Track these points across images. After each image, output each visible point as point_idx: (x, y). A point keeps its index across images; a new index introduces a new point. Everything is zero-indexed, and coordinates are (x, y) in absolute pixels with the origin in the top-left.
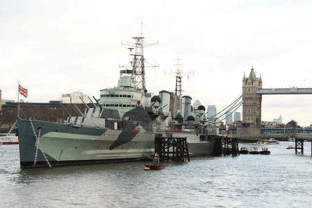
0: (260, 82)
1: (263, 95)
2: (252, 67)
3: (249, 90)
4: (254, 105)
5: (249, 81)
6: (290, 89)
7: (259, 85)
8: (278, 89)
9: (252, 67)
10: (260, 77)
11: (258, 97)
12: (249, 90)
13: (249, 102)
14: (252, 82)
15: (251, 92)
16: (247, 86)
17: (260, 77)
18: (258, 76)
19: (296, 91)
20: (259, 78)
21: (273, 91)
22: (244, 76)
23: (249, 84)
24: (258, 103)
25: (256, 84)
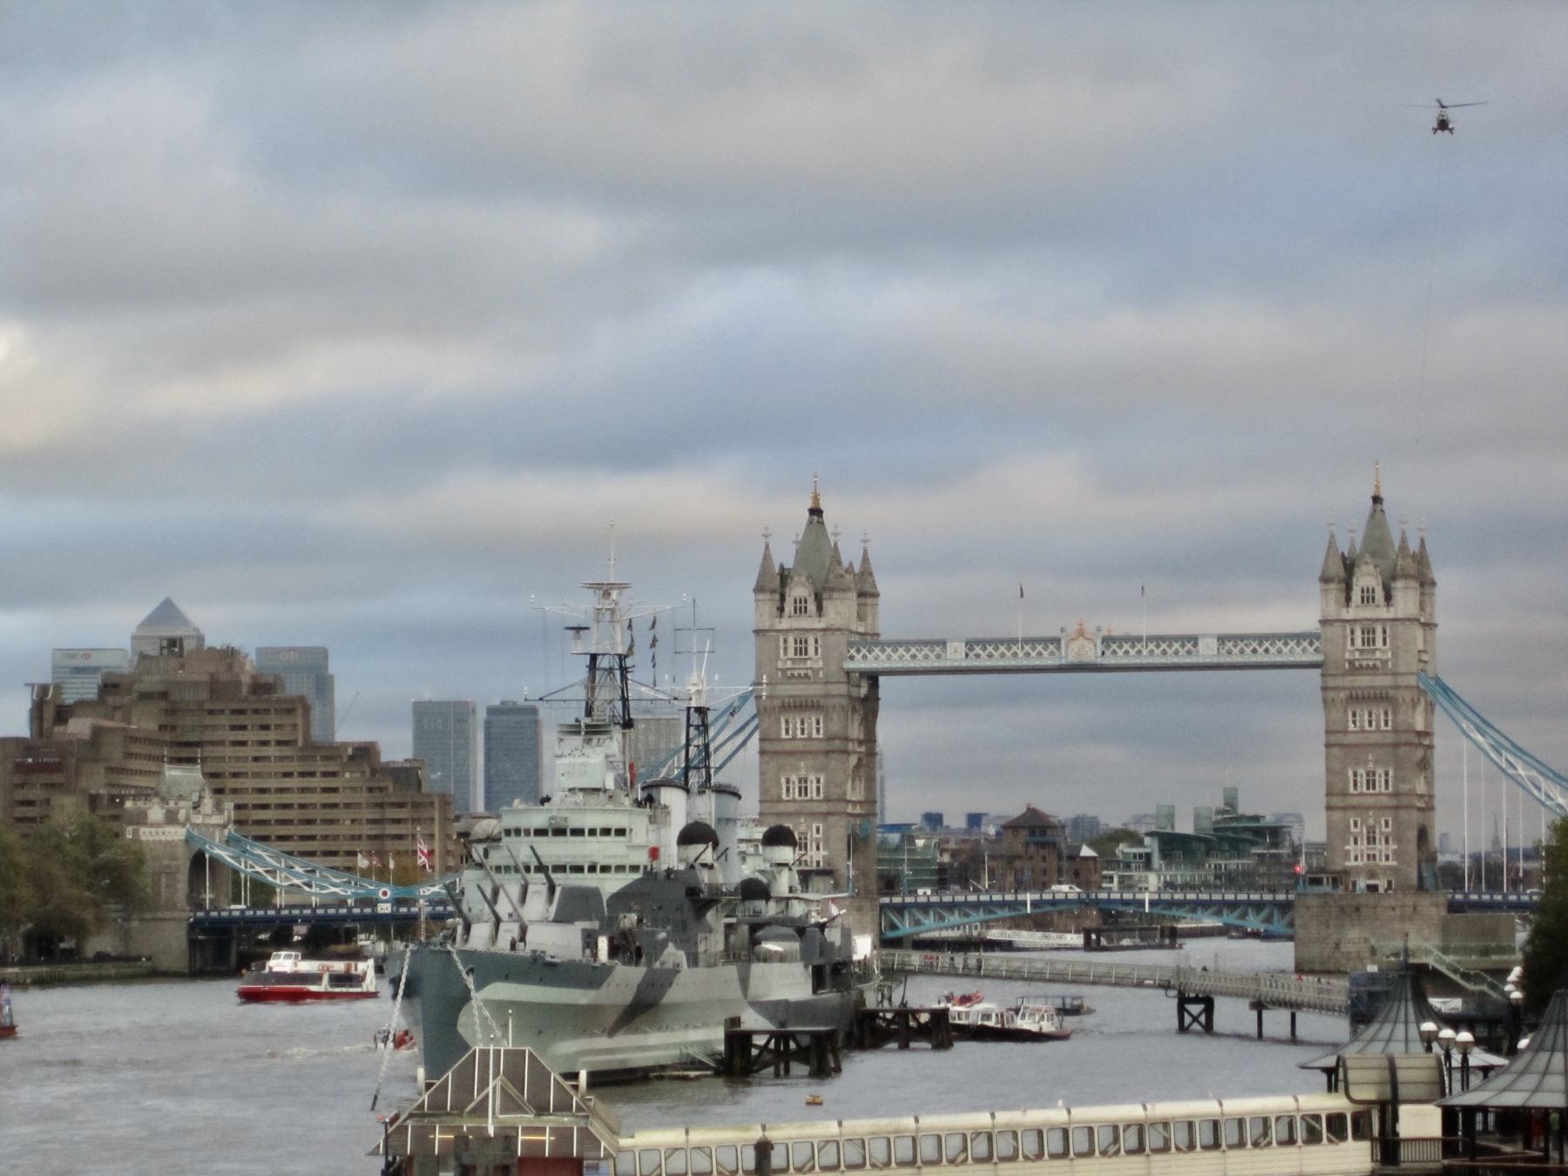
0: (867, 594)
1: (882, 679)
2: (816, 499)
3: (801, 650)
4: (834, 747)
5: (799, 590)
6: (1056, 641)
7: (861, 617)
8: (984, 643)
9: (816, 499)
10: (865, 559)
11: (854, 692)
12: (801, 650)
13: (811, 727)
14: (818, 599)
15: (815, 662)
16: (785, 624)
17: (865, 559)
18: (850, 555)
19: (1090, 652)
20: (857, 570)
21: (955, 654)
22: (767, 558)
23: (801, 609)
24: (856, 731)
25: (840, 611)
